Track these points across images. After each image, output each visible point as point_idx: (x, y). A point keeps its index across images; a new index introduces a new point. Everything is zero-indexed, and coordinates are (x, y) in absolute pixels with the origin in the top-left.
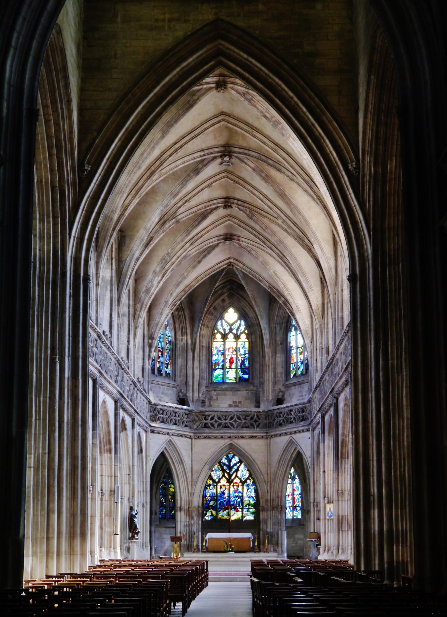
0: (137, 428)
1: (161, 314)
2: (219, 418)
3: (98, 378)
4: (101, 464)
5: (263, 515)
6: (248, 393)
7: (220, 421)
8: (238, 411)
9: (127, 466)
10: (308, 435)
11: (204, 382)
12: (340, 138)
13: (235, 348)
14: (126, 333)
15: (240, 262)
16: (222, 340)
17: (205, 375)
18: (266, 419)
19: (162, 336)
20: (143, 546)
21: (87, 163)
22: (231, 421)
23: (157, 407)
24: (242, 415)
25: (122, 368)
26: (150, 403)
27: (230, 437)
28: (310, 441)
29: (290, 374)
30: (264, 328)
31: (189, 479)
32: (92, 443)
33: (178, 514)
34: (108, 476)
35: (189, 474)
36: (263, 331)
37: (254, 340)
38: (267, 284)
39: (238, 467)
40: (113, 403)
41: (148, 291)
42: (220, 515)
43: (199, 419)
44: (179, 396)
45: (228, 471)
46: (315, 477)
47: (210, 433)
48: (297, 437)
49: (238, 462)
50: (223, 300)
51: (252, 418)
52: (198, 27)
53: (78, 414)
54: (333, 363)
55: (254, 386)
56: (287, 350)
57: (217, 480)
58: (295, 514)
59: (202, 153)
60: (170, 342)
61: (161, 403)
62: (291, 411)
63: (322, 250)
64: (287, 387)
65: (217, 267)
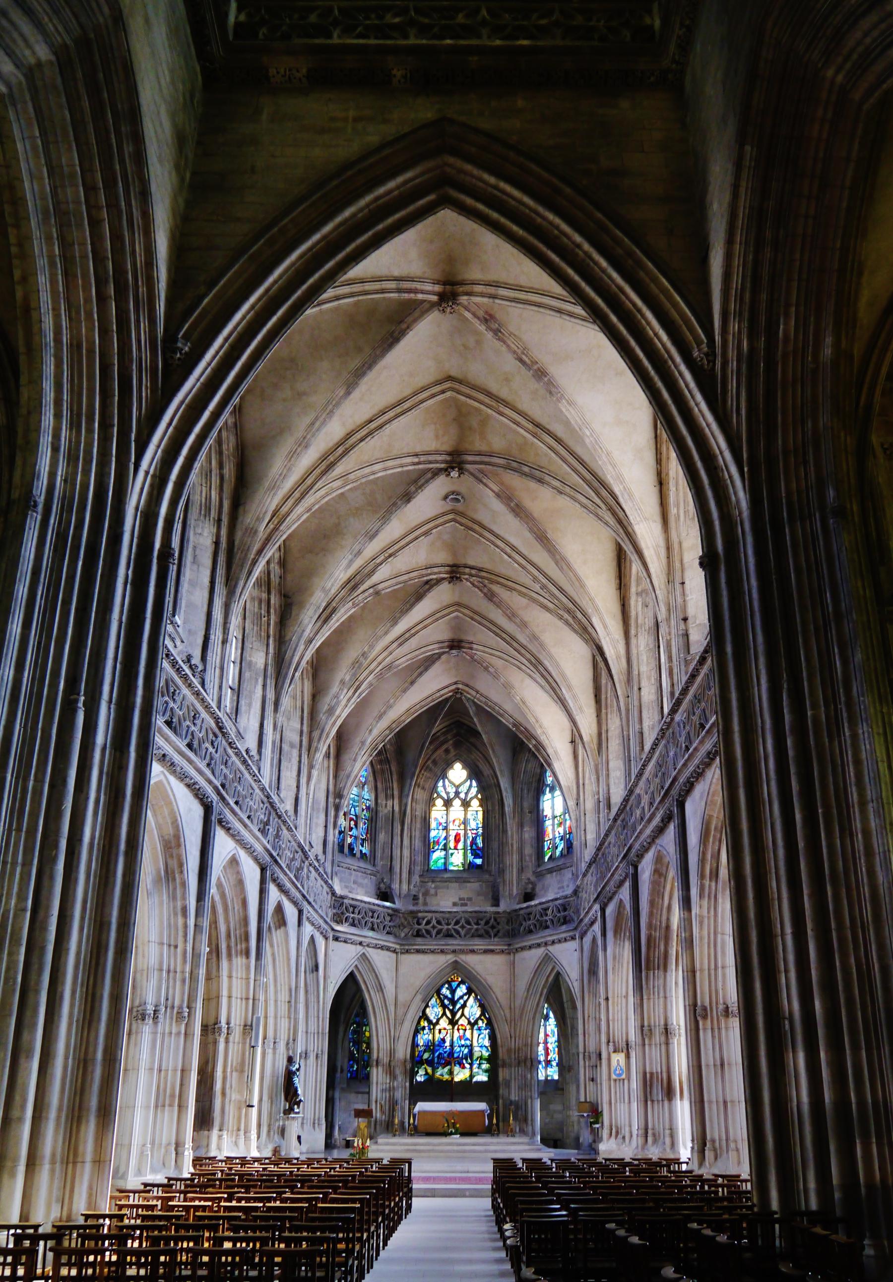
0: (308, 929)
1: (355, 760)
2: (439, 922)
3: (214, 804)
4: (230, 977)
5: (503, 1074)
6: (481, 886)
7: (440, 927)
8: (467, 912)
9: (287, 987)
10: (573, 945)
11: (418, 869)
12: (675, 305)
13: (462, 819)
14: (295, 773)
15: (472, 688)
16: (445, 808)
17: (419, 858)
18: (508, 923)
19: (356, 798)
20: (314, 1123)
21: (183, 337)
22: (456, 927)
23: (346, 901)
24: (472, 917)
25: (277, 814)
26: (333, 893)
27: (454, 951)
28: (576, 955)
29: (543, 857)
30: (506, 789)
31: (392, 1017)
32: (195, 925)
33: (375, 1070)
34: (242, 999)
35: (392, 1008)
36: (504, 794)
37: (490, 808)
38: (511, 720)
39: (465, 1002)
40: (258, 871)
41: (331, 711)
42: (439, 1073)
43: (409, 923)
44: (379, 889)
45: (451, 1007)
46: (586, 1012)
47: (425, 945)
48: (554, 949)
49: (465, 994)
50: (447, 751)
51: (487, 923)
52: (407, 129)
53: (120, 827)
54: (628, 808)
55: (490, 875)
56: (538, 821)
57: (434, 1021)
58: (549, 1073)
59: (416, 460)
60: (368, 808)
61: (351, 896)
62: (547, 909)
63: (605, 627)
64: (540, 875)
65: (438, 695)
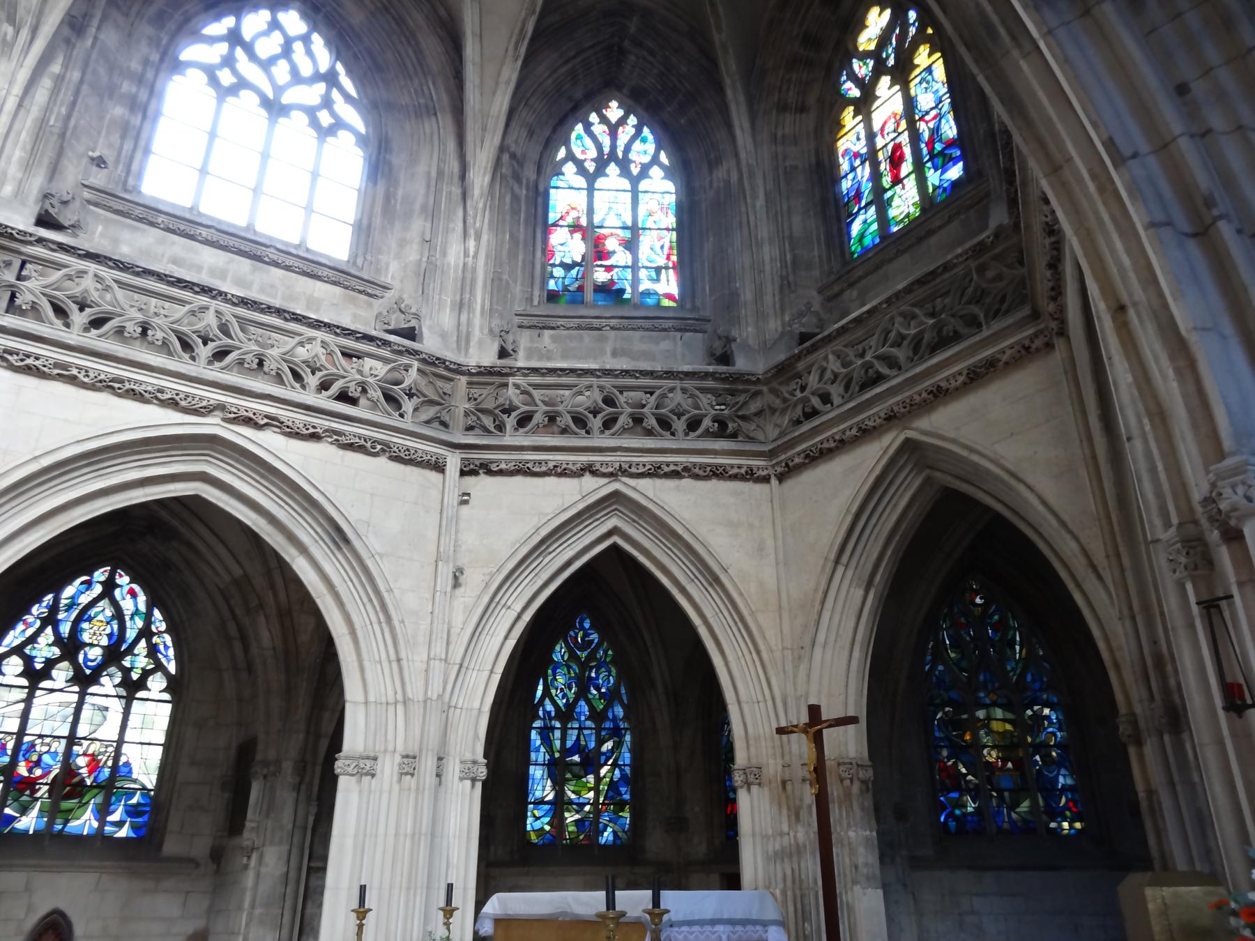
8: (898, 295)
